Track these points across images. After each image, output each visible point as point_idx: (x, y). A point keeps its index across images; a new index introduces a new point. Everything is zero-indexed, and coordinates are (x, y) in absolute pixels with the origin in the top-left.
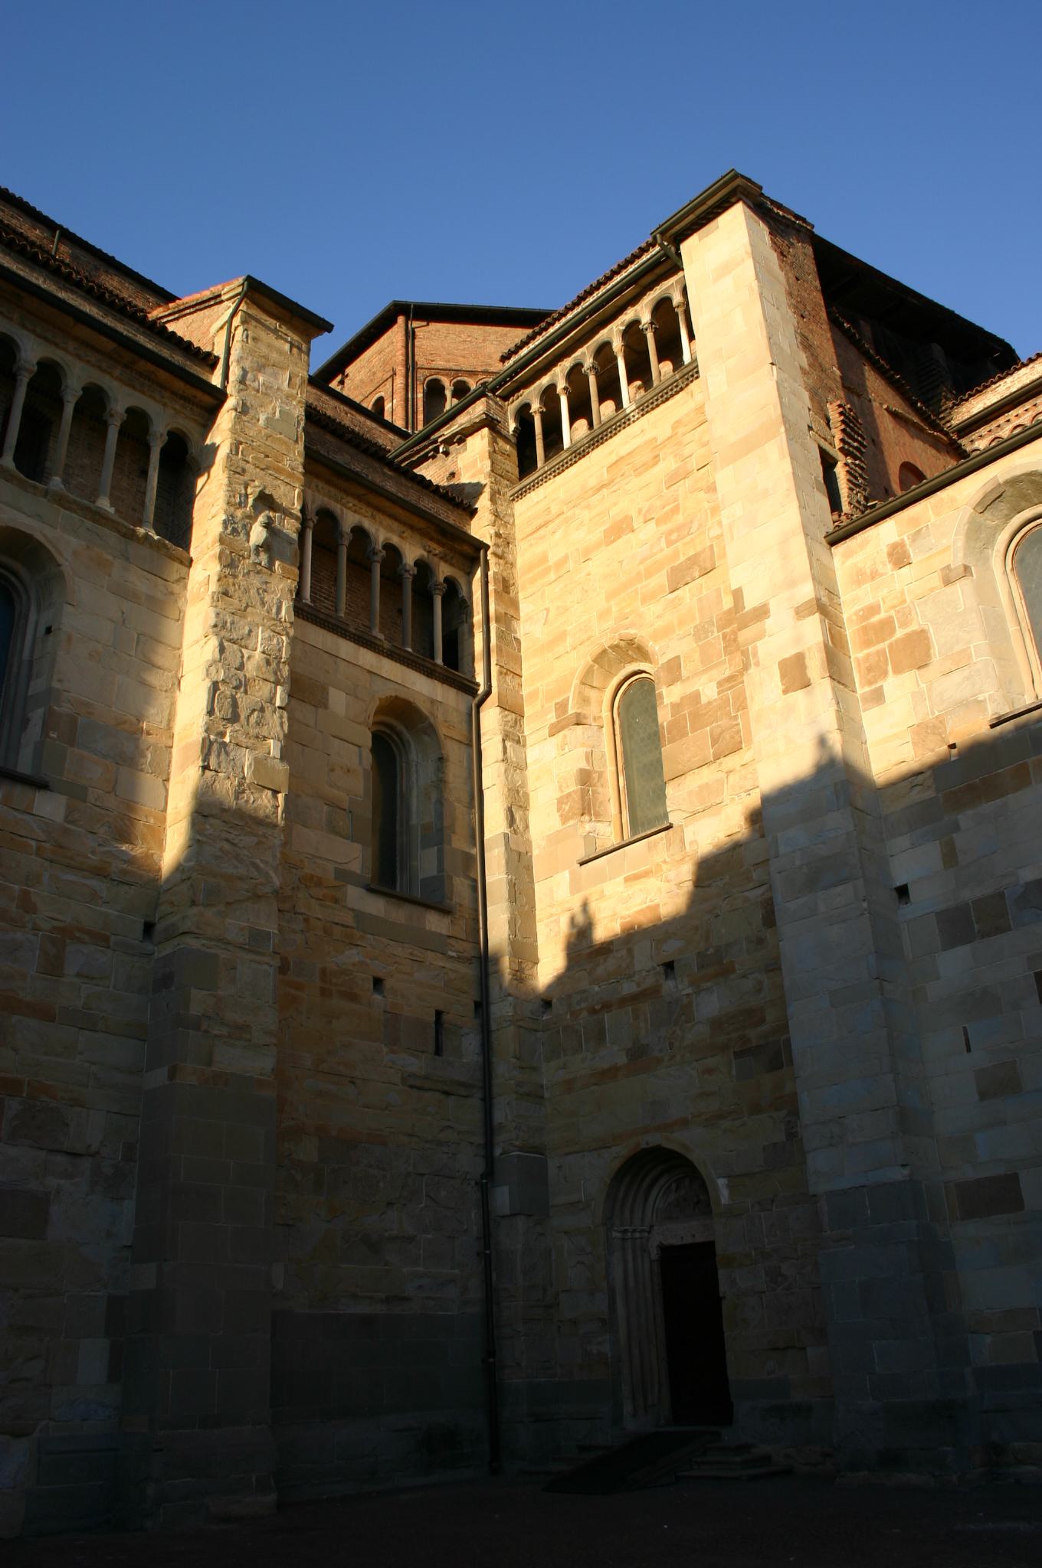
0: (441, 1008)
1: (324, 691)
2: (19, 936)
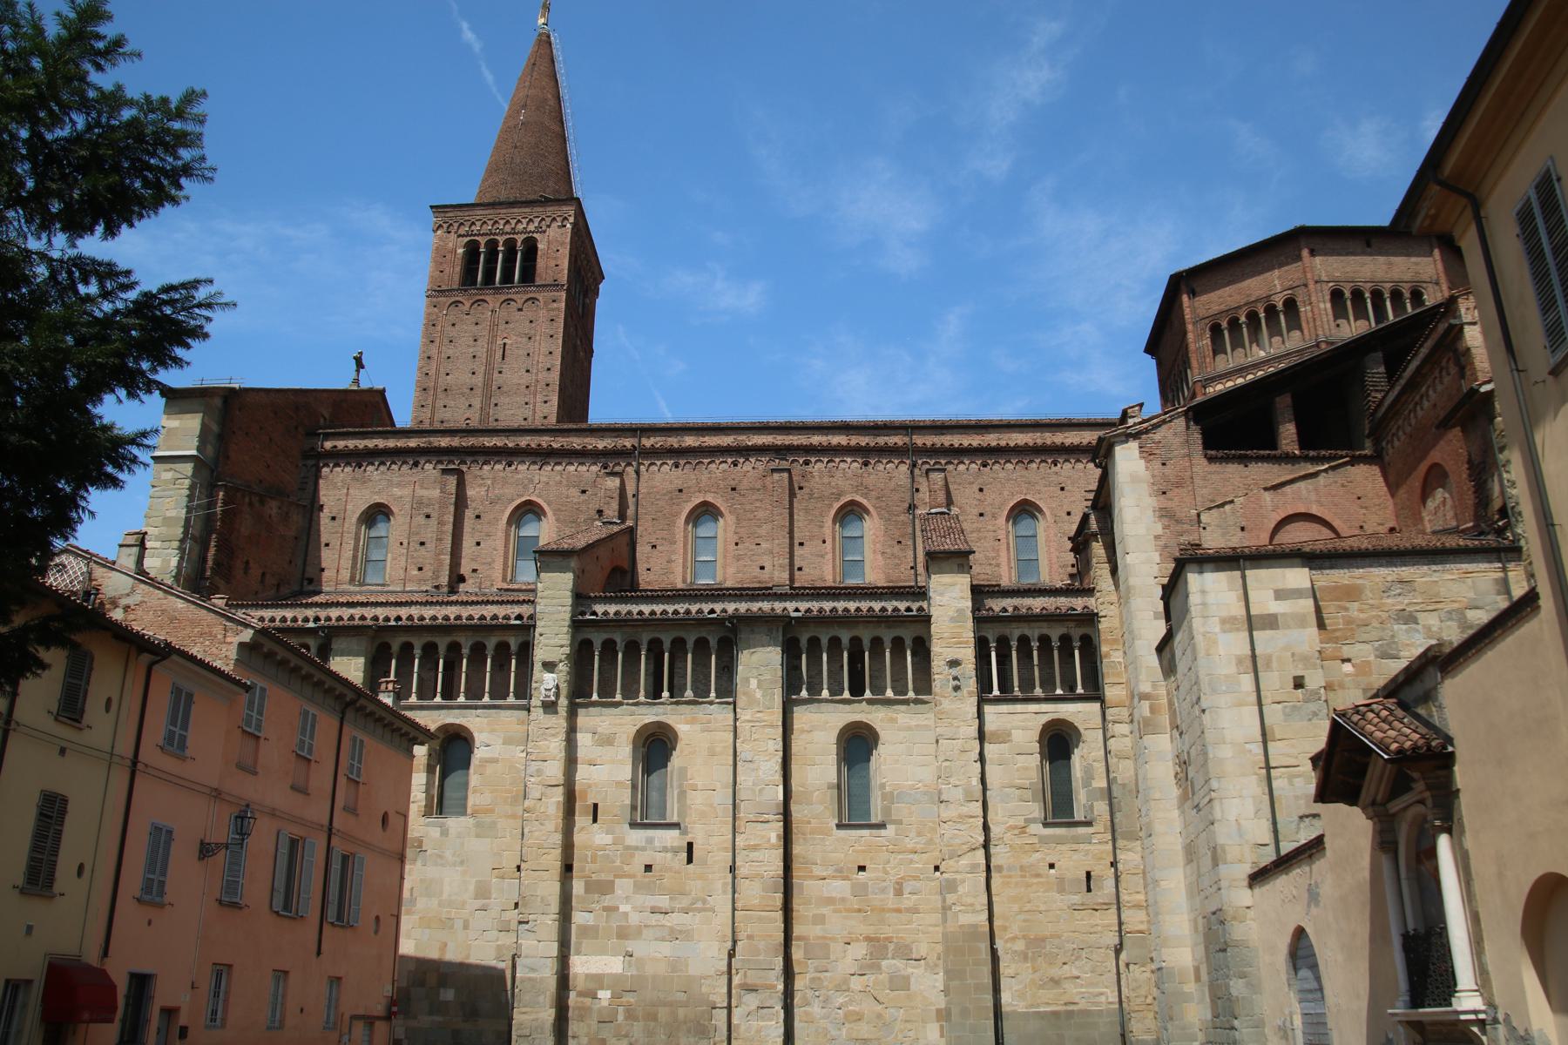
0: (1089, 869)
1: (1009, 734)
2: (885, 884)
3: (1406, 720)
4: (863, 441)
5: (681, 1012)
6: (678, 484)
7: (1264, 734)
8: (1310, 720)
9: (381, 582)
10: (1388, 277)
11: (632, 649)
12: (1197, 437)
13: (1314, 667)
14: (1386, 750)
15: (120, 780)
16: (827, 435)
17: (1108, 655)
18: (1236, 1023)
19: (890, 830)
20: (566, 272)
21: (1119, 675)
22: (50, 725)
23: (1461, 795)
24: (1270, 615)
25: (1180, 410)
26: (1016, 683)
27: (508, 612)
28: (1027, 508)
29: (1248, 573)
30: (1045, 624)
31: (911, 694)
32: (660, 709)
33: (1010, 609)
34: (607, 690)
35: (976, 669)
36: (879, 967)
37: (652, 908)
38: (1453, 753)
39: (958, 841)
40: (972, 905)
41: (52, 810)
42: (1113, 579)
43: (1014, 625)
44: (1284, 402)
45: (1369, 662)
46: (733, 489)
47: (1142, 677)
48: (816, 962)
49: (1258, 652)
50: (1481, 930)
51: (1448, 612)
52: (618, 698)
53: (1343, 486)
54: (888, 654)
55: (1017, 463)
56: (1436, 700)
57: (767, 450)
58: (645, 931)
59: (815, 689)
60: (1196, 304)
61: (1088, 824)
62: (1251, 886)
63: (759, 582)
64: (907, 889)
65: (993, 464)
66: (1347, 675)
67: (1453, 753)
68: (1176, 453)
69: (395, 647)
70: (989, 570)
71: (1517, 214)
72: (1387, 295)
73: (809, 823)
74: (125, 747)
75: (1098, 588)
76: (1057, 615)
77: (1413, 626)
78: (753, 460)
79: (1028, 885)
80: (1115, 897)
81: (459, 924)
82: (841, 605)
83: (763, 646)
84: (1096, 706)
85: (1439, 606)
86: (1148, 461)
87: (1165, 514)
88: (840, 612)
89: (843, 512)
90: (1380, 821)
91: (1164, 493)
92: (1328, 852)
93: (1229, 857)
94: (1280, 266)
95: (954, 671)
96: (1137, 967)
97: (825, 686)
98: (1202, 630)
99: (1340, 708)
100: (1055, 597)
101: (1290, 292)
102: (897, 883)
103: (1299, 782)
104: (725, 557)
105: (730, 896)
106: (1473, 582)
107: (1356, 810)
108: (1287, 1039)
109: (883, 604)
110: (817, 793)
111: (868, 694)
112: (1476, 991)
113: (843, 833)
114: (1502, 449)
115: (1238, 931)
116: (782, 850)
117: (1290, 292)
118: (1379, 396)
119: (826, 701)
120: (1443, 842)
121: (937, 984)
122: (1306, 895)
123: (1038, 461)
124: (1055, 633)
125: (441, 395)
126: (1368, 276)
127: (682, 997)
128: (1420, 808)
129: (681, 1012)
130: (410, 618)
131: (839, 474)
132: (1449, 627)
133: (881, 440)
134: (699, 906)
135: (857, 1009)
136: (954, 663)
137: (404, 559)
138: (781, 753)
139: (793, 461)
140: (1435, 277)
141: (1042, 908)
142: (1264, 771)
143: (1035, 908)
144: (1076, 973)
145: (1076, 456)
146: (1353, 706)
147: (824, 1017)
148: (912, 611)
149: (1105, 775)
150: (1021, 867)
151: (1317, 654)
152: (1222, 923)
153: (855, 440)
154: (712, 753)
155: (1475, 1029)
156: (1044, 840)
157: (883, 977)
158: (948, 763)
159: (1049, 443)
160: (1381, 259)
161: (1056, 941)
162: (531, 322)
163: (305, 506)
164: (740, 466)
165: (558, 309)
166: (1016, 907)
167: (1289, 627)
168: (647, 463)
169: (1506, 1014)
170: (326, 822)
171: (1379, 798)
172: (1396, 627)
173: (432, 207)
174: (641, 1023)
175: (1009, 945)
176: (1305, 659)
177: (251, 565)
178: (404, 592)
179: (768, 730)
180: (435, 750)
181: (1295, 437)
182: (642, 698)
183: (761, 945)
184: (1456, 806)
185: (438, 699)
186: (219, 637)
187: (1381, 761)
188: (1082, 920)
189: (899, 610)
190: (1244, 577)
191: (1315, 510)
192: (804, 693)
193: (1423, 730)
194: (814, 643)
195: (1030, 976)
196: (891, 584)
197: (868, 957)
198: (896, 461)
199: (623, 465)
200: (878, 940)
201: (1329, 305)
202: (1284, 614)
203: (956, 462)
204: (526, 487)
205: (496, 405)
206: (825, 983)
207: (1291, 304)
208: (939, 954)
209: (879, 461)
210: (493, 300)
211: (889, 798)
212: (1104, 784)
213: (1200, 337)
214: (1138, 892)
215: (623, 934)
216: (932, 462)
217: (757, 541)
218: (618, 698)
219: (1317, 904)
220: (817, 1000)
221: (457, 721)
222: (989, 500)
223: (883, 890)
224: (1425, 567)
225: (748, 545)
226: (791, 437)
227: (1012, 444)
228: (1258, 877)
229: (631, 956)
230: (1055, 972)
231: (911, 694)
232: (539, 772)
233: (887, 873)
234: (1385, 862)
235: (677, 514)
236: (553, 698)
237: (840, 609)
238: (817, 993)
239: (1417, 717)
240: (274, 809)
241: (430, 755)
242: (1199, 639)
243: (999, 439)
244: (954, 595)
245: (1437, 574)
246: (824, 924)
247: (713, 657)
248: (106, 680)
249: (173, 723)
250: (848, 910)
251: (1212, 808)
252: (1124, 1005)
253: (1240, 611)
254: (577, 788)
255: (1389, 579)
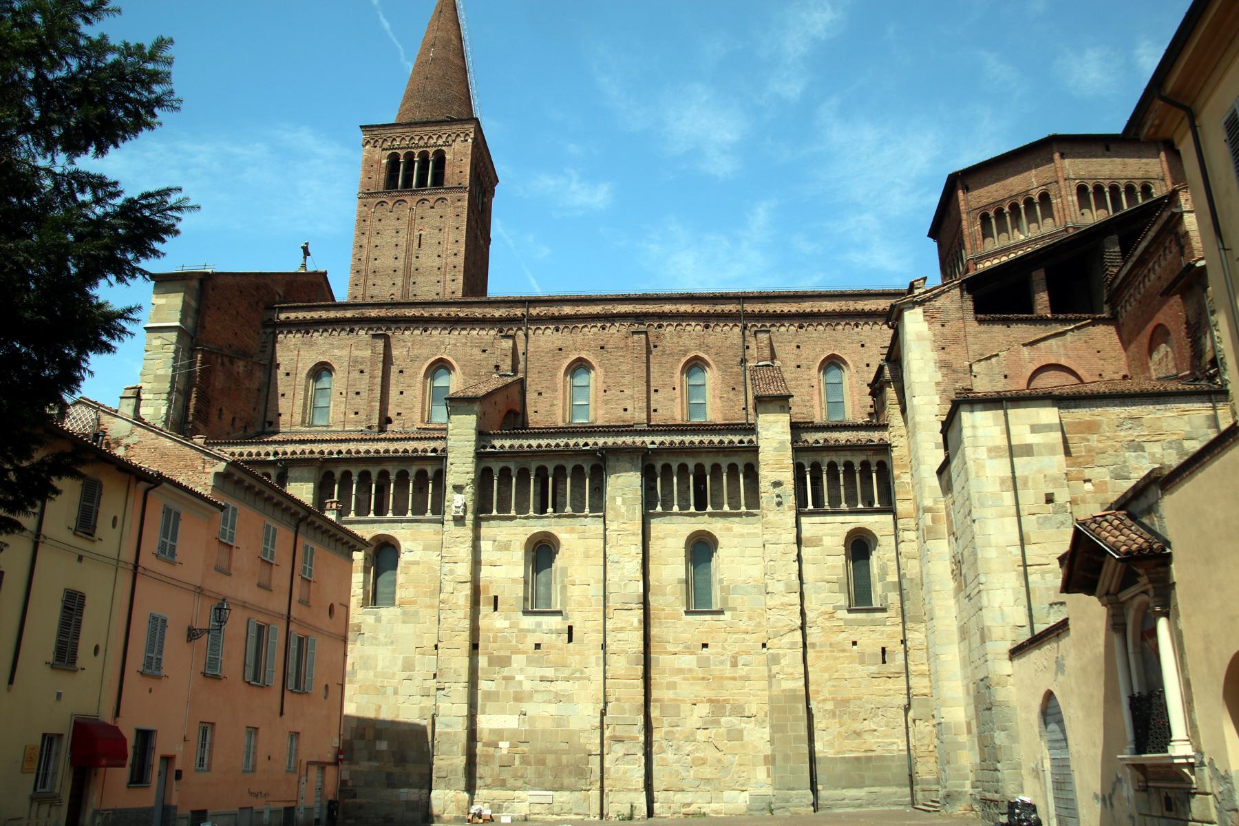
1: (821, 540)
2: (722, 658)
3: (1133, 528)
4: (705, 308)
5: (564, 758)
6: (559, 344)
7: (1022, 539)
8: (1058, 528)
9: (326, 424)
10: (1124, 174)
11: (523, 475)
12: (969, 304)
13: (1062, 486)
14: (1117, 551)
15: (125, 580)
16: (676, 304)
17: (899, 477)
18: (999, 766)
19: (727, 616)
20: (468, 177)
21: (907, 493)
22: (69, 538)
23: (1176, 587)
24: (1027, 445)
25: (956, 282)
26: (826, 499)
27: (426, 446)
28: (835, 361)
29: (1009, 411)
30: (848, 453)
31: (743, 509)
32: (545, 521)
33: (822, 441)
34: (504, 507)
35: (795, 489)
36: (719, 723)
37: (541, 677)
38: (1170, 554)
39: (780, 624)
40: (792, 674)
41: (73, 604)
42: (903, 418)
43: (824, 454)
44: (1039, 276)
45: (1105, 482)
46: (602, 348)
47: (926, 494)
48: (670, 719)
49: (1017, 474)
50: (1191, 693)
51: (1169, 442)
52: (513, 513)
53: (1086, 342)
54: (725, 477)
55: (827, 325)
56: (1158, 511)
57: (628, 317)
58: (537, 697)
59: (667, 505)
60: (969, 198)
61: (884, 610)
62: (1011, 659)
63: (623, 421)
64: (740, 663)
65: (808, 326)
66: (1088, 492)
67: (1170, 554)
68: (952, 316)
69: (338, 474)
70: (804, 410)
71: (1225, 123)
72: (1122, 189)
73: (664, 610)
74: (128, 555)
75: (891, 424)
76: (858, 446)
77: (1141, 453)
78: (617, 325)
79: (836, 659)
80: (904, 667)
81: (390, 691)
82: (687, 439)
83: (626, 471)
84: (890, 517)
85: (1162, 437)
86: (930, 323)
87: (944, 365)
88: (507, 448)
89: (690, 364)
90: (1112, 608)
91: (943, 348)
92: (1072, 632)
93: (994, 636)
94: (1037, 166)
95: (777, 491)
96: (921, 722)
97: (676, 502)
98: (973, 457)
99: (1081, 518)
100: (857, 431)
101: (1044, 187)
102: (733, 657)
103: (1049, 577)
104: (596, 401)
105: (602, 668)
106: (1189, 418)
107: (1093, 599)
108: (1039, 779)
109: (721, 437)
110: (670, 586)
111: (709, 509)
112: (1187, 740)
113: (690, 618)
114: (1213, 312)
115: (1000, 694)
116: (642, 632)
117: (1044, 187)
118: (1115, 270)
119: (677, 514)
120: (1162, 625)
121: (764, 736)
122: (1054, 666)
123: (843, 323)
124: (857, 460)
125: (371, 276)
126: (1107, 174)
127: (565, 746)
128: (1145, 597)
129: (564, 758)
130: (349, 452)
131: (685, 335)
132: (1170, 454)
133: (719, 308)
134: (578, 676)
135: (702, 755)
136: (777, 484)
137: (343, 405)
138: (641, 556)
139: (649, 326)
140: (1161, 174)
141: (847, 676)
142: (1022, 568)
143: (841, 677)
144: (874, 727)
145: (874, 320)
146: (1091, 517)
147: (678, 762)
148: (744, 443)
149: (896, 572)
150: (831, 645)
151: (1064, 476)
152: (988, 687)
153: (698, 308)
154: (587, 557)
155: (1186, 770)
156: (848, 623)
157: (722, 730)
158: (772, 563)
159: (852, 309)
160: (1118, 160)
161: (858, 702)
162: (441, 217)
163: (265, 365)
164: (607, 329)
165: (462, 206)
166: (826, 676)
167: (1041, 454)
168: (533, 328)
169: (1211, 759)
170: (285, 611)
171: (1112, 590)
172: (1127, 454)
173: (361, 127)
174: (533, 767)
175: (821, 705)
176: (1055, 480)
177: (224, 411)
178: (343, 431)
179: (630, 538)
180: (370, 555)
181: (1047, 304)
182: (531, 513)
183: (627, 706)
184: (1172, 595)
185: (372, 515)
186: (200, 468)
187: (1114, 560)
188: (879, 685)
189: (733, 442)
190: (1006, 415)
191: (1063, 362)
192: (659, 509)
193: (1147, 536)
194: (667, 469)
195: (838, 730)
196: (727, 422)
197: (710, 715)
198: (731, 325)
199: (515, 329)
200: (718, 701)
201: (1075, 198)
202: (1038, 444)
203: (778, 325)
204: (438, 348)
205: (414, 283)
206: (677, 736)
207: (1045, 198)
208: (766, 713)
209: (717, 325)
210: (411, 200)
211: (726, 590)
212: (896, 579)
213: (972, 224)
214: (923, 664)
215: (518, 698)
216: (759, 325)
217: (622, 389)
218: (513, 513)
219: (1063, 673)
220: (670, 748)
221: (387, 533)
222: (805, 355)
223: (722, 663)
224: (1151, 407)
225: (614, 392)
226: (647, 306)
227: (823, 311)
228: (1017, 652)
229: (525, 715)
230: (857, 726)
231: (743, 509)
232: (452, 572)
233: (724, 649)
234: (1117, 639)
235: (558, 368)
236: (462, 514)
237: (687, 442)
238: (670, 743)
239: (1142, 525)
240: (245, 602)
241: (366, 559)
242: (970, 464)
243: (812, 307)
244: (777, 430)
245: (1161, 412)
246: (676, 689)
247: (587, 480)
248: (112, 503)
249: (165, 535)
250: (694, 678)
251: (980, 597)
252: (912, 752)
253: (1002, 441)
254: (481, 584)
255: (1122, 416)
